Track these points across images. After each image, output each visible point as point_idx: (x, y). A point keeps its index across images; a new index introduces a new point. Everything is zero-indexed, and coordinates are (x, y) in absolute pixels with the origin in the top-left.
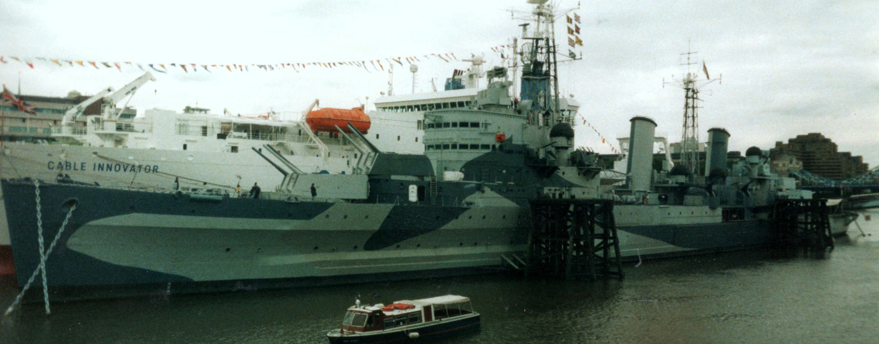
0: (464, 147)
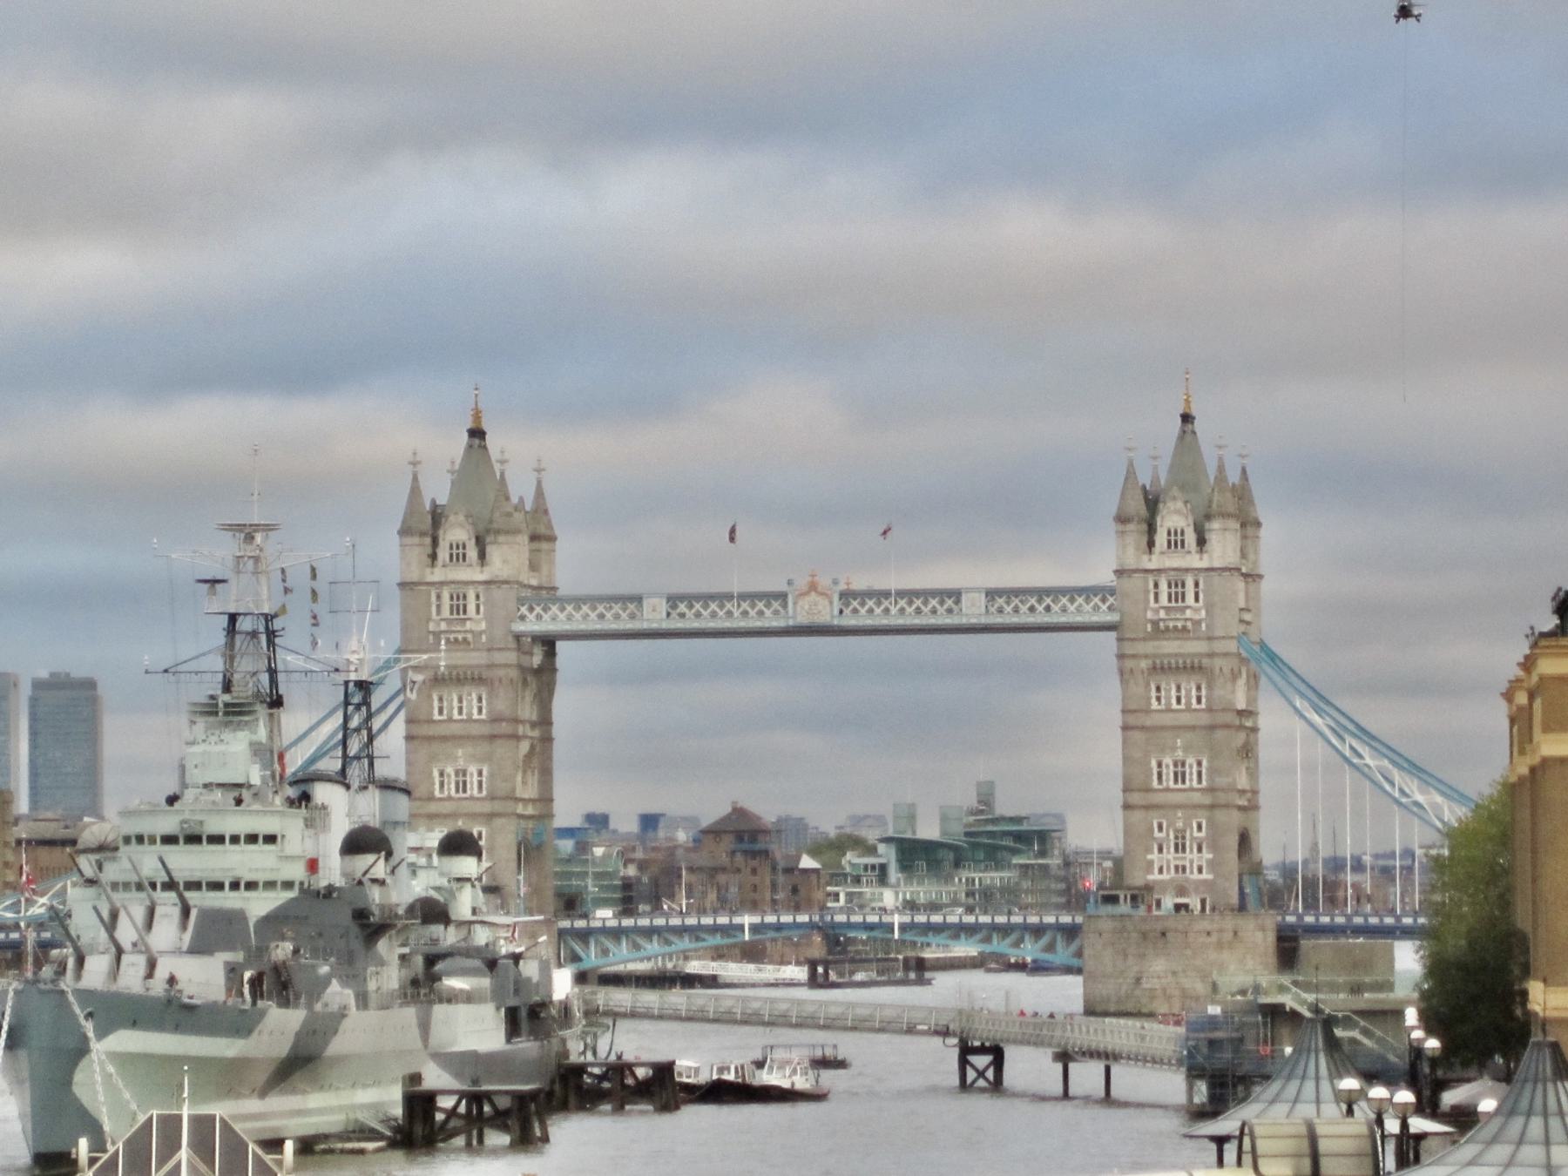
0: (251, 886)
